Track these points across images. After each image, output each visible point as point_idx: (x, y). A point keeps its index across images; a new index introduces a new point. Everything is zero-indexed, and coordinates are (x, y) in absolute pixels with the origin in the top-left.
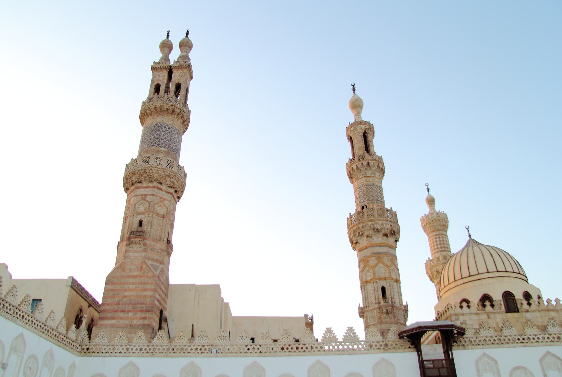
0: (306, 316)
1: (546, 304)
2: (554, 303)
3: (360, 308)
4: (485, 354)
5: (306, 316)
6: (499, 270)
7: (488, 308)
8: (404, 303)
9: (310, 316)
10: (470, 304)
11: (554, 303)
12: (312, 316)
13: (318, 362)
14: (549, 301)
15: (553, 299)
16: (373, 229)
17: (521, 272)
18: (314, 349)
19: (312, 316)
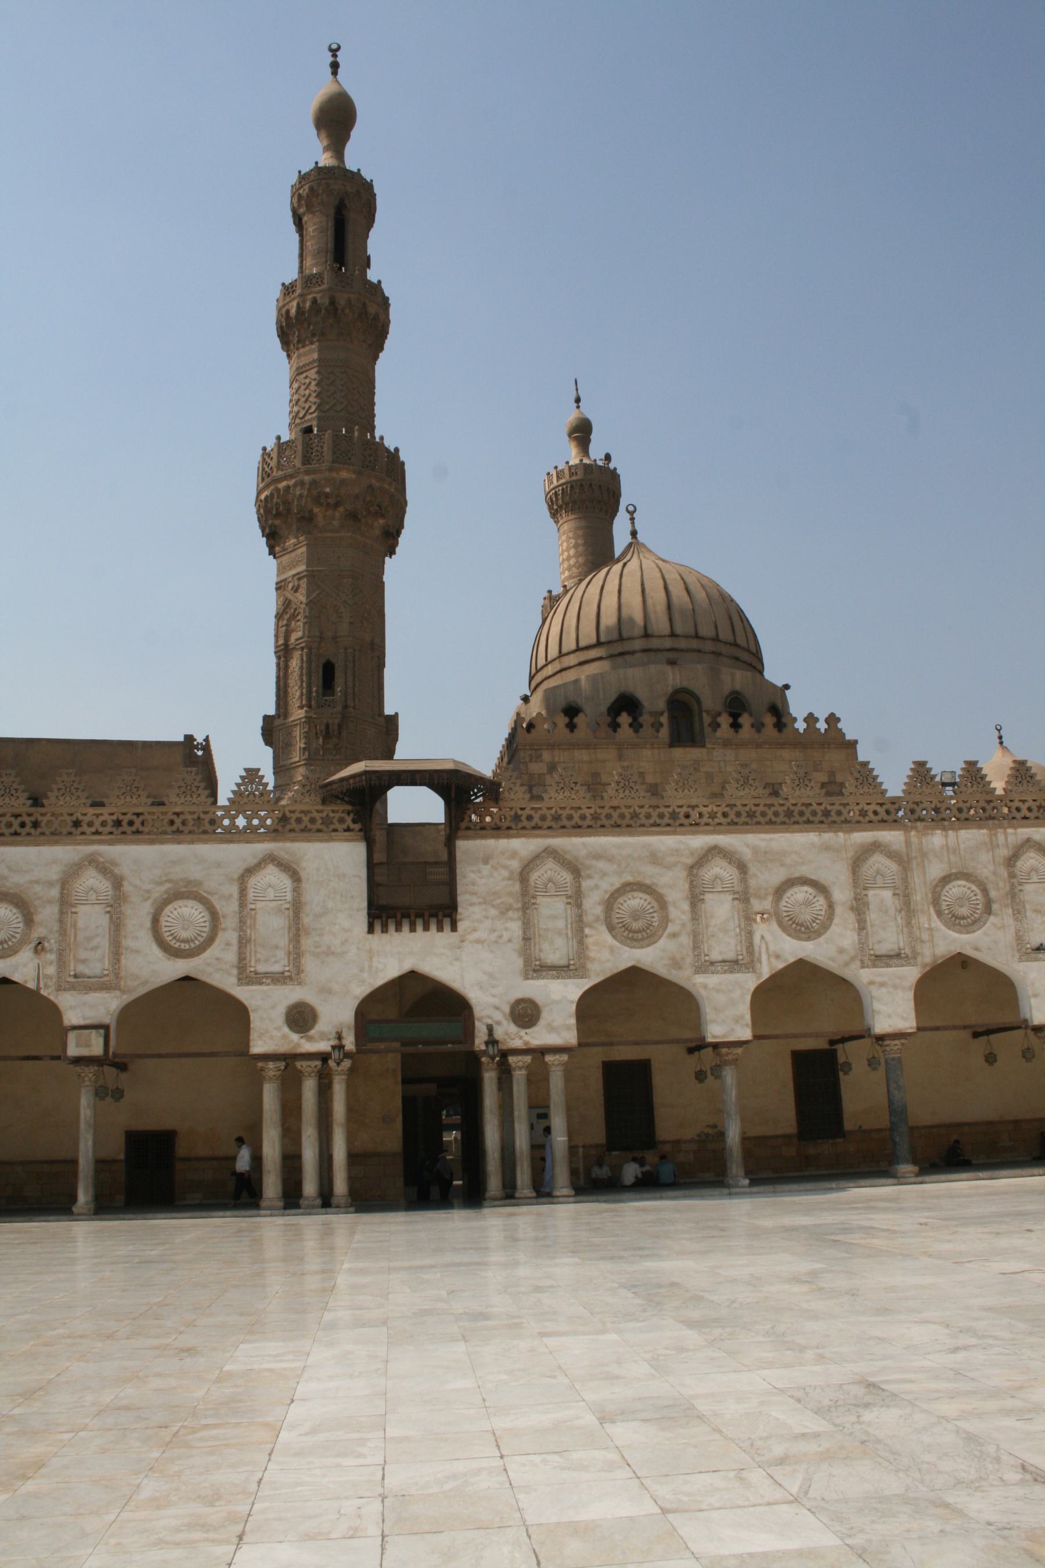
0: (189, 738)
1: (801, 726)
2: (822, 726)
3: (266, 718)
4: (552, 853)
5: (189, 738)
6: (679, 630)
7: (625, 731)
8: (388, 711)
9: (200, 739)
10: (575, 720)
11: (822, 726)
12: (207, 739)
13: (92, 860)
14: (811, 719)
15: (822, 715)
16: (335, 504)
17: (741, 641)
18: (85, 828)
19: (207, 739)
